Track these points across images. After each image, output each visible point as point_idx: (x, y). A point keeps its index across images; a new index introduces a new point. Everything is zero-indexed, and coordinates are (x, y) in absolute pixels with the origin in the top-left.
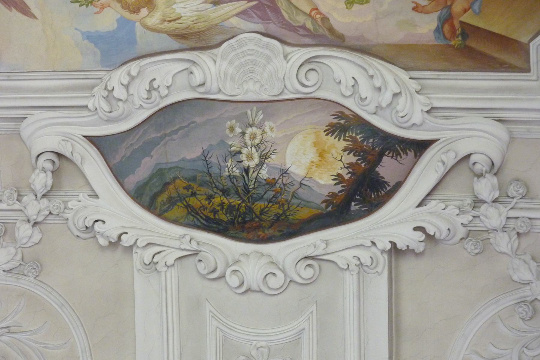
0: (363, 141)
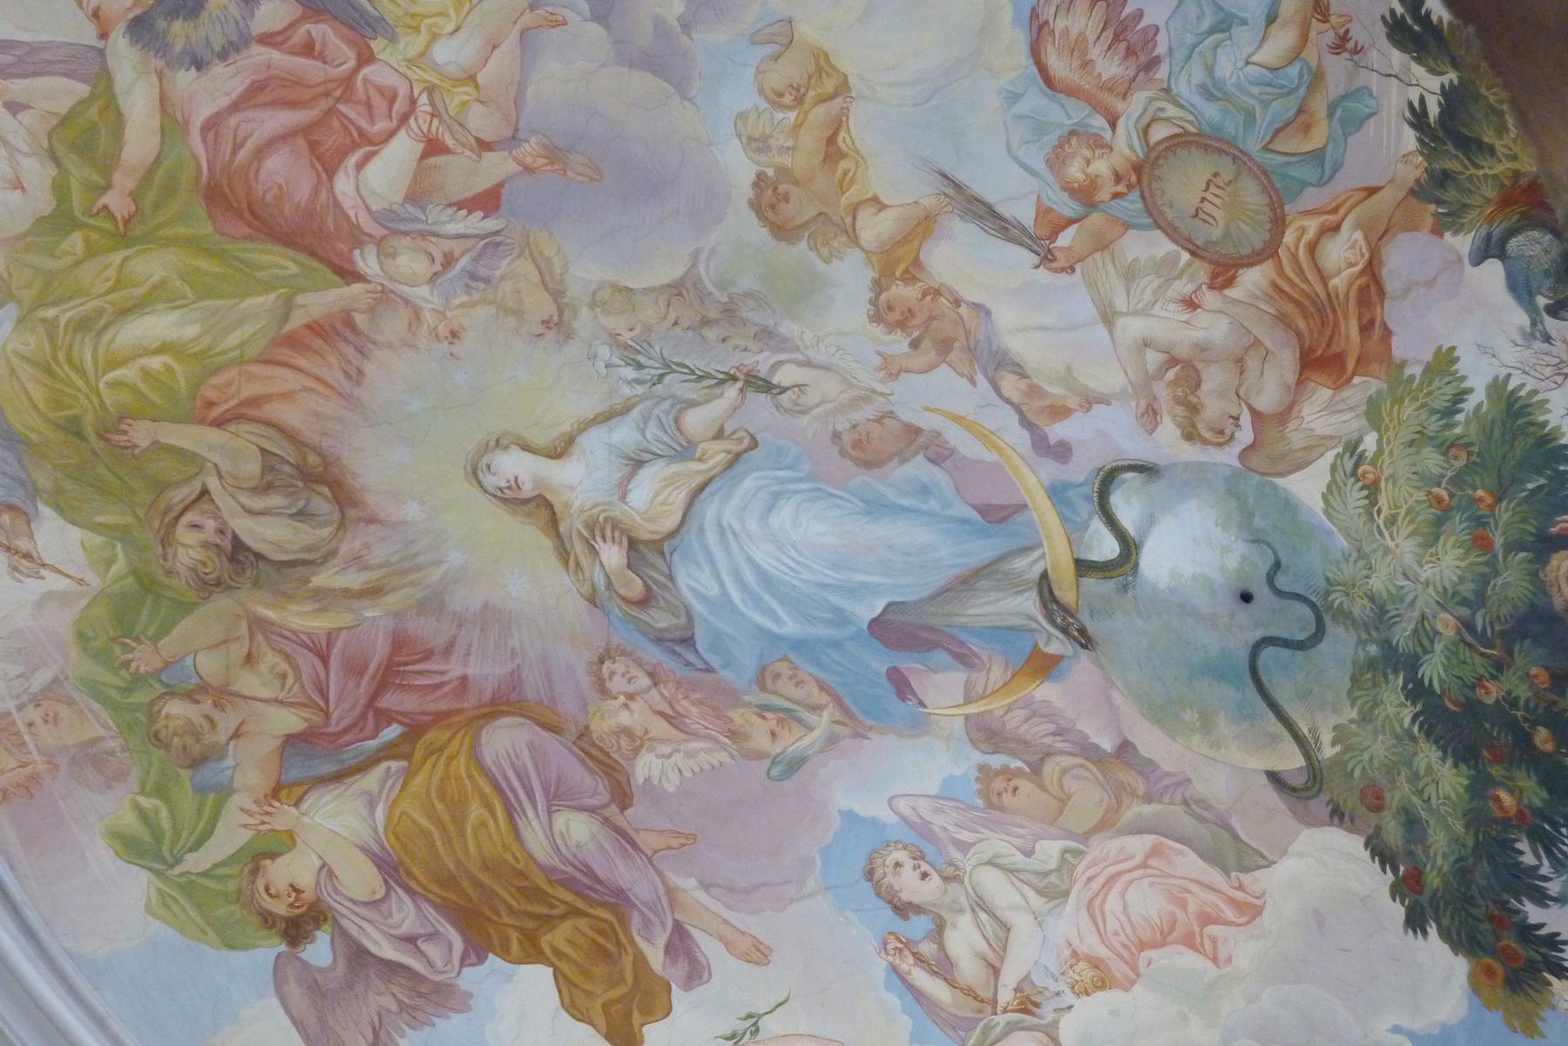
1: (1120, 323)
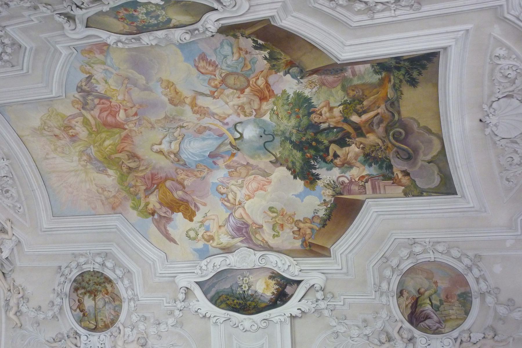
0: (280, 281)
1: (229, 103)
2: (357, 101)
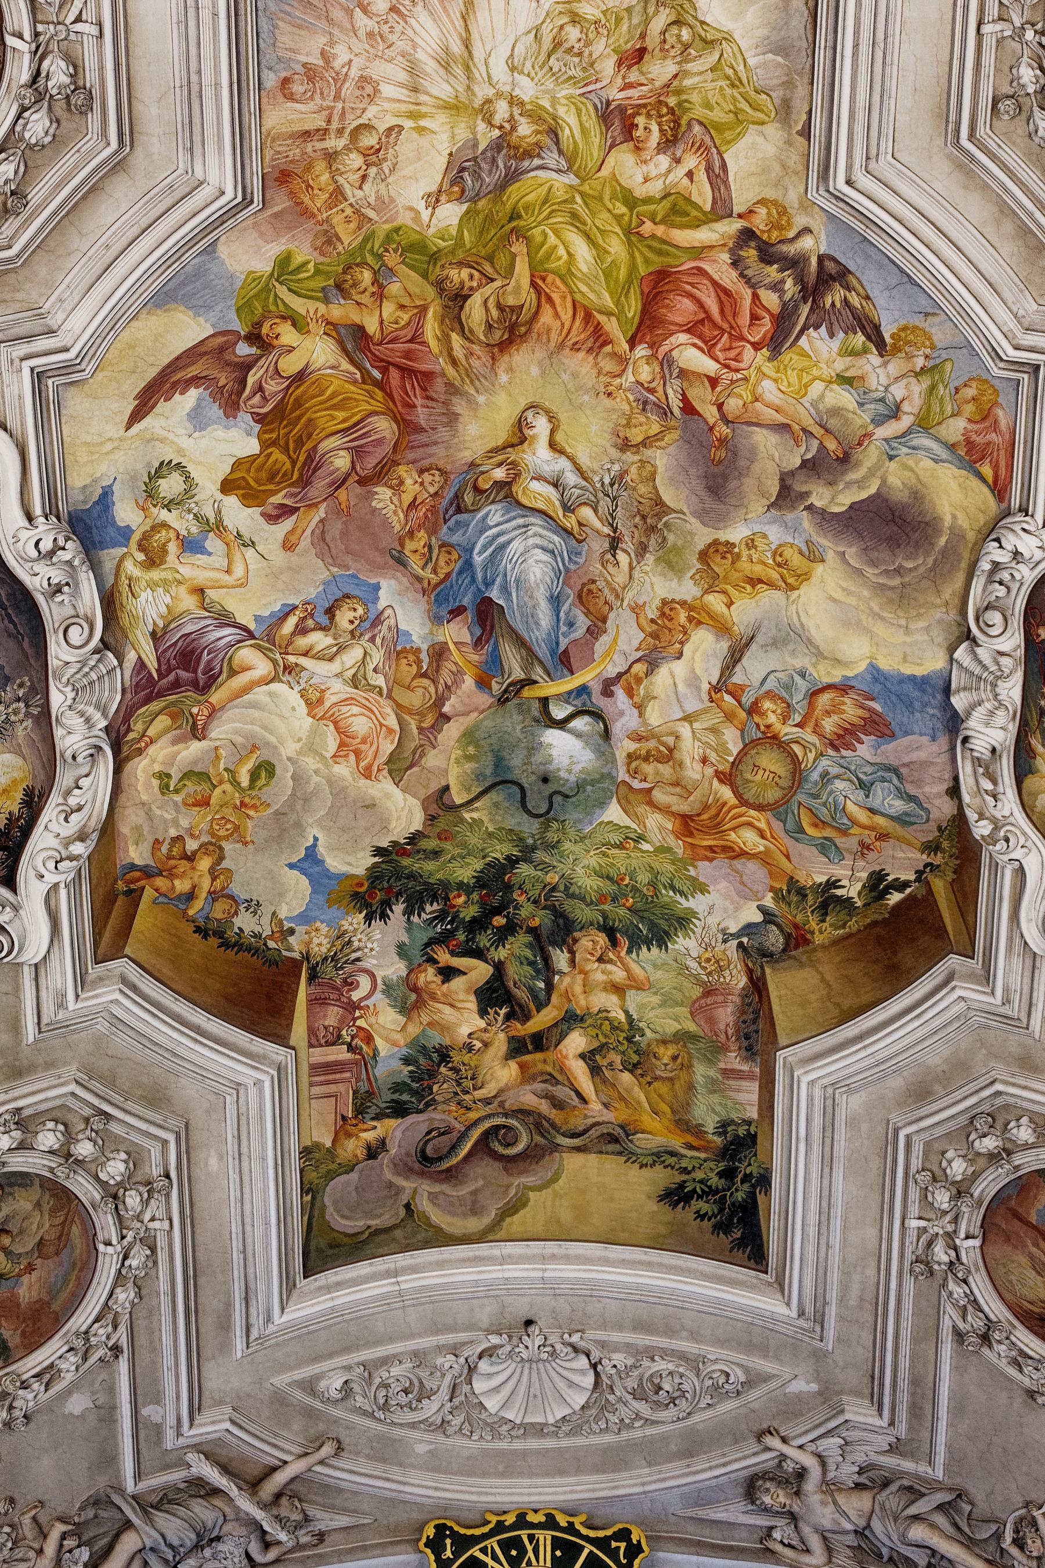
1: (686, 724)
2: (635, 1058)
